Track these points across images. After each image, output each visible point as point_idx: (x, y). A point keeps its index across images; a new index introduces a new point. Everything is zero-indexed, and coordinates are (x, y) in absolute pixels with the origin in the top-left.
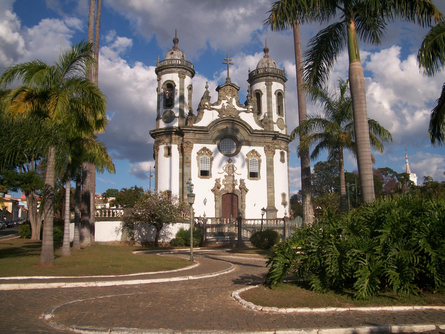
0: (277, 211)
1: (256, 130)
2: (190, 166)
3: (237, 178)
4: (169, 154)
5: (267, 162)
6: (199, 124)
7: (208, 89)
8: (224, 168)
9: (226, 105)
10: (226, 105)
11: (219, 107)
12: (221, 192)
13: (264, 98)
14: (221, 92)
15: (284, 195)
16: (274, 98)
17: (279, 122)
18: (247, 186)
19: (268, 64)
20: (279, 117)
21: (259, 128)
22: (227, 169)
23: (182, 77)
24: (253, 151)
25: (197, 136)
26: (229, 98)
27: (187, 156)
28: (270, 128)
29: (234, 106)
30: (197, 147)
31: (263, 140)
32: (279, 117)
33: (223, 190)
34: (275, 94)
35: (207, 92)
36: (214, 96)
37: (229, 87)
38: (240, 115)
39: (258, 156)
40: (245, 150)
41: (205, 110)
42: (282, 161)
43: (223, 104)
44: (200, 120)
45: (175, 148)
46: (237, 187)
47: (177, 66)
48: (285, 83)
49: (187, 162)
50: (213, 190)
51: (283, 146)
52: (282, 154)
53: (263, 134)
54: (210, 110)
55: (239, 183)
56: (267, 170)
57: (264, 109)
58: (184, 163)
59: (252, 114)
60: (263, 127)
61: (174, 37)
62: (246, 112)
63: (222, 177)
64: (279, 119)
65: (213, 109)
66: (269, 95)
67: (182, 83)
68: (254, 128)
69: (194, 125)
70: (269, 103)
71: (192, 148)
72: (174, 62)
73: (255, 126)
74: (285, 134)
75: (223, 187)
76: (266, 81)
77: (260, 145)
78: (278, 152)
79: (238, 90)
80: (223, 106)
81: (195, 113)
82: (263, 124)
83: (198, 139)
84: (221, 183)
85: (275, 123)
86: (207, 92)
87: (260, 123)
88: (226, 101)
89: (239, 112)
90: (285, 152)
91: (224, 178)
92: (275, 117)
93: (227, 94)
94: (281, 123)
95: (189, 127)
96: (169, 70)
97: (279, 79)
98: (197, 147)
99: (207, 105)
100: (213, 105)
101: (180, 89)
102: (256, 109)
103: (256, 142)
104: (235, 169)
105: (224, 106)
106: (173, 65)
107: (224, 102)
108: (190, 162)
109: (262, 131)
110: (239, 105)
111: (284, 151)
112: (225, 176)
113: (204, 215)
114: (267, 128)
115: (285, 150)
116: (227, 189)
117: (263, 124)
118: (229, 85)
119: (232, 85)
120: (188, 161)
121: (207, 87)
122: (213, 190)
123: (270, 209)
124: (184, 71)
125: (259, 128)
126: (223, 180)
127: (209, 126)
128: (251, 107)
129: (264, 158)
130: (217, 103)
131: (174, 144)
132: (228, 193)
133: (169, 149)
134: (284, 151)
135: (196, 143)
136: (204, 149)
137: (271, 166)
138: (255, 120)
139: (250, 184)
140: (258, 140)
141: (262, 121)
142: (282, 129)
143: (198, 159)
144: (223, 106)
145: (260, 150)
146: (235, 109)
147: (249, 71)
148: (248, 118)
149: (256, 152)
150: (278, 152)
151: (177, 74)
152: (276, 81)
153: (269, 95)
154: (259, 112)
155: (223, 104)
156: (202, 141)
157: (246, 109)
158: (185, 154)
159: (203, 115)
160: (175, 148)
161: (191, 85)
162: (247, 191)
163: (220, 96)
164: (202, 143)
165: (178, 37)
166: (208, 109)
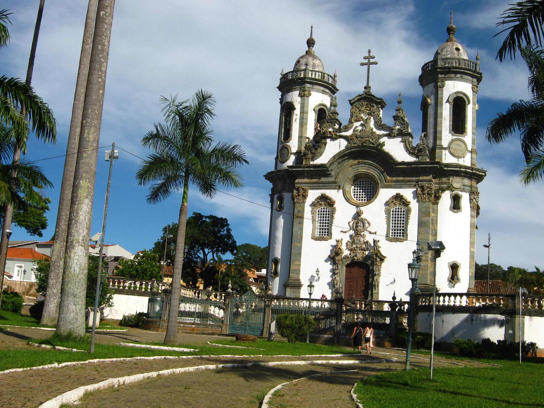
1: (403, 163)
2: (301, 223)
3: (370, 239)
8: (351, 224)
9: (360, 128)
11: (349, 133)
12: (344, 260)
13: (431, 111)
17: (451, 146)
18: (383, 251)
20: (454, 137)
22: (355, 225)
24: (398, 197)
27: (299, 208)
32: (454, 137)
33: (346, 257)
39: (406, 204)
40: (385, 194)
44: (321, 155)
51: (455, 185)
60: (417, 157)
63: (346, 238)
64: (453, 141)
69: (311, 163)
71: (305, 197)
74: (469, 165)
84: (344, 247)
85: (445, 149)
88: (362, 122)
89: (380, 137)
91: (349, 239)
94: (458, 147)
97: (459, 76)
98: (313, 195)
99: (330, 132)
101: (301, 113)
104: (367, 225)
105: (357, 131)
108: (302, 217)
111: (461, 193)
112: (351, 236)
113: (394, 298)
115: (463, 191)
120: (299, 215)
124: (308, 85)
129: (414, 206)
130: (346, 129)
131: (288, 192)
133: (281, 199)
134: (461, 193)
135: (312, 189)
136: (324, 198)
137: (426, 219)
139: (385, 247)
142: (458, 157)
143: (313, 213)
146: (373, 133)
152: (451, 79)
155: (356, 127)
156: (321, 185)
158: (297, 205)
159: (325, 148)
162: (382, 259)
164: (321, 189)
165: (314, 37)
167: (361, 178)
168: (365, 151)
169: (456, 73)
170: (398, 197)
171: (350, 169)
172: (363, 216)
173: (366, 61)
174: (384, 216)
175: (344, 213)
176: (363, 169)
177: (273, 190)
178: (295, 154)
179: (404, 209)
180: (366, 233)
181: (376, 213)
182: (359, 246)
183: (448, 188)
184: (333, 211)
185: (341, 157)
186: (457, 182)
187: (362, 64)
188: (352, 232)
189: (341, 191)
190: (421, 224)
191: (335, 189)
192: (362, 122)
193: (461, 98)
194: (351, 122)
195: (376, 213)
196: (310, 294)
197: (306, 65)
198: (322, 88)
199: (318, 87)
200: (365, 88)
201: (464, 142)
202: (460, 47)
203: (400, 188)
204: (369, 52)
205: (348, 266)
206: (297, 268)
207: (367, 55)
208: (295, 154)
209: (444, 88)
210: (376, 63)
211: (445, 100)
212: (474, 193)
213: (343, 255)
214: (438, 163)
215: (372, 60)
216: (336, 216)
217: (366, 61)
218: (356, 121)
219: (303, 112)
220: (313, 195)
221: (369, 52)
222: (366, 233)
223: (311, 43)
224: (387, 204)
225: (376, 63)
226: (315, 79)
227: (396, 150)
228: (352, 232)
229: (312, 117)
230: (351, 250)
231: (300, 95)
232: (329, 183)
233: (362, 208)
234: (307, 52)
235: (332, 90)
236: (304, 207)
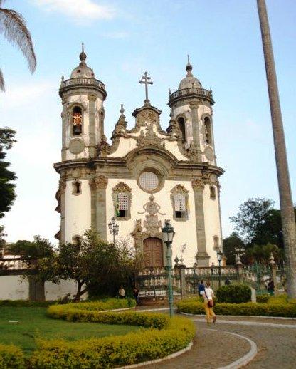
0: (209, 257)
2: (104, 206)
3: (162, 219)
4: (78, 191)
6: (114, 155)
7: (124, 113)
9: (145, 132)
10: (145, 132)
11: (138, 135)
13: (189, 124)
14: (140, 116)
15: (216, 239)
16: (201, 123)
19: (193, 84)
21: (185, 159)
23: (92, 99)
24: (179, 186)
25: (113, 169)
26: (149, 124)
27: (101, 193)
28: (197, 159)
29: (155, 134)
30: (113, 182)
31: (189, 173)
33: (144, 234)
34: (202, 119)
35: (123, 117)
36: (131, 122)
37: (148, 111)
39: (185, 191)
40: (170, 185)
41: (121, 139)
42: (213, 197)
43: (142, 131)
44: (115, 150)
45: (85, 184)
47: (87, 87)
48: (212, 107)
49: (101, 201)
50: (133, 234)
51: (213, 180)
52: (212, 189)
53: (189, 167)
54: (126, 138)
55: (163, 226)
57: (190, 139)
58: (97, 203)
59: (176, 143)
60: (189, 157)
61: (81, 52)
62: (169, 140)
63: (143, 218)
65: (131, 137)
66: (195, 120)
67: (92, 106)
68: (179, 159)
71: (106, 183)
72: (83, 82)
73: (180, 157)
75: (144, 230)
76: (190, 103)
78: (207, 187)
79: (159, 114)
80: (142, 133)
81: (109, 142)
83: (114, 173)
84: (142, 225)
86: (123, 117)
87: (186, 152)
90: (216, 187)
92: (202, 148)
93: (147, 120)
95: (101, 158)
96: (78, 90)
98: (113, 182)
100: (130, 132)
102: (181, 136)
103: (182, 175)
106: (81, 85)
107: (143, 128)
108: (104, 201)
109: (188, 162)
112: (147, 217)
114: (194, 159)
119: (152, 109)
121: (122, 111)
122: (133, 234)
123: (202, 255)
124: (94, 92)
125: (185, 159)
126: (145, 221)
127: (126, 156)
128: (175, 134)
131: (84, 179)
132: (150, 237)
133: (78, 185)
136: (122, 185)
138: (180, 150)
139: (174, 224)
140: (184, 172)
141: (187, 150)
143: (113, 198)
144: (142, 133)
145: (187, 185)
147: (170, 93)
148: (173, 148)
149: (183, 188)
150: (207, 187)
151: (86, 96)
154: (184, 141)
157: (168, 137)
160: (85, 184)
161: (103, 110)
163: (138, 122)
166: (124, 137)
168: (151, 150)
169: (204, 100)
170: (179, 186)
171: (141, 163)
172: (154, 201)
173: (144, 80)
174: (170, 201)
176: (151, 164)
178: (89, 147)
180: (157, 214)
183: (208, 183)
184: (130, 197)
185: (136, 153)
186: (213, 178)
187: (141, 82)
188: (147, 214)
189: (135, 181)
190: (196, 209)
191: (130, 178)
194: (137, 126)
195: (164, 198)
200: (145, 101)
203: (180, 180)
204: (146, 74)
205: (145, 240)
207: (144, 75)
208: (89, 147)
209: (199, 109)
210: (151, 83)
212: (219, 186)
215: (148, 81)
217: (144, 80)
221: (146, 74)
222: (157, 214)
223: (83, 57)
224: (172, 191)
225: (151, 83)
228: (147, 214)
230: (147, 228)
231: (89, 98)
233: (154, 195)
234: (81, 64)
236: (105, 193)
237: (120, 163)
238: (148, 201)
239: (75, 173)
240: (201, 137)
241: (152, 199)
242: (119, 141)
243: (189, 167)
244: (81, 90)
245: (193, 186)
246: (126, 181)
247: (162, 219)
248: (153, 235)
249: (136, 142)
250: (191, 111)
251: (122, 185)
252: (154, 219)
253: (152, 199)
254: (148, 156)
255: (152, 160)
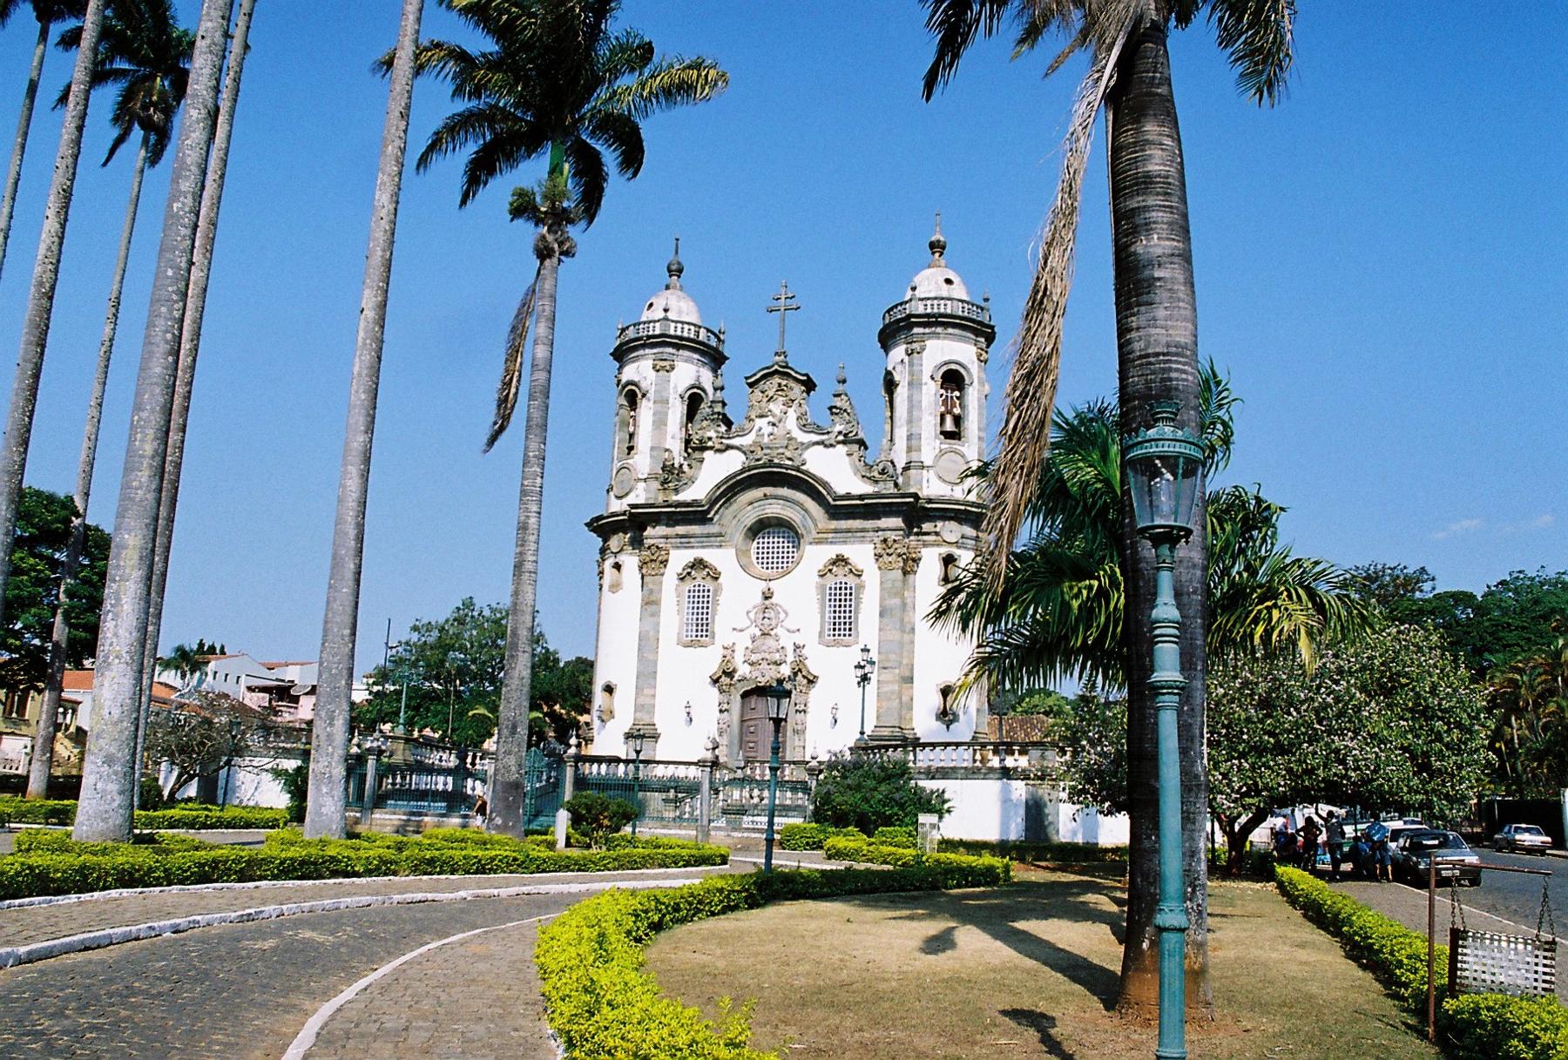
1: (848, 496)
2: (656, 614)
3: (787, 641)
5: (882, 589)
6: (686, 496)
8: (752, 615)
9: (767, 429)
16: (931, 391)
18: (813, 667)
24: (840, 560)
25: (680, 530)
31: (869, 524)
37: (776, 380)
38: (808, 455)
40: (816, 556)
41: (708, 455)
46: (786, 671)
53: (867, 509)
55: (790, 658)
56: (881, 615)
58: (650, 603)
63: (743, 642)
64: (942, 453)
65: (729, 447)
67: (663, 386)
68: (841, 491)
69: (675, 498)
70: (913, 405)
71: (665, 563)
75: (743, 670)
77: (862, 540)
82: (875, 474)
88: (770, 419)
98: (679, 559)
104: (782, 616)
108: (657, 603)
109: (861, 497)
110: (804, 427)
111: (956, 552)
116: (755, 674)
117: (875, 474)
118: (776, 372)
120: (653, 598)
124: (670, 350)
128: (838, 428)
130: (743, 433)
133: (617, 566)
136: (699, 564)
145: (861, 554)
151: (650, 363)
152: (937, 336)
153: (914, 384)
166: (711, 448)
167: (770, 526)
170: (840, 560)
172: (773, 600)
174: (813, 596)
175: (738, 592)
176: (774, 509)
177: (603, 551)
179: (852, 581)
180: (778, 631)
181: (800, 589)
182: (766, 656)
186: (951, 531)
192: (770, 419)
193: (957, 371)
195: (800, 589)
196: (638, 752)
197: (666, 310)
198: (696, 356)
199: (687, 353)
201: (963, 456)
202: (952, 275)
206: (648, 701)
211: (926, 378)
213: (736, 677)
214: (916, 496)
216: (722, 599)
218: (761, 416)
219: (663, 401)
220: (679, 559)
226: (681, 338)
227: (837, 471)
229: (677, 411)
230: (752, 664)
232: (708, 536)
233: (772, 584)
235: (715, 359)
237: (696, 515)
238: (759, 599)
239: (615, 542)
240: (929, 425)
241: (767, 596)
242: (702, 461)
243: (867, 509)
244: (641, 352)
245: (878, 556)
246: (708, 555)
247: (787, 641)
248: (763, 681)
249: (743, 458)
250: (906, 359)
251: (699, 564)
252: (770, 642)
253: (767, 596)
254: (769, 490)
255: (776, 497)
